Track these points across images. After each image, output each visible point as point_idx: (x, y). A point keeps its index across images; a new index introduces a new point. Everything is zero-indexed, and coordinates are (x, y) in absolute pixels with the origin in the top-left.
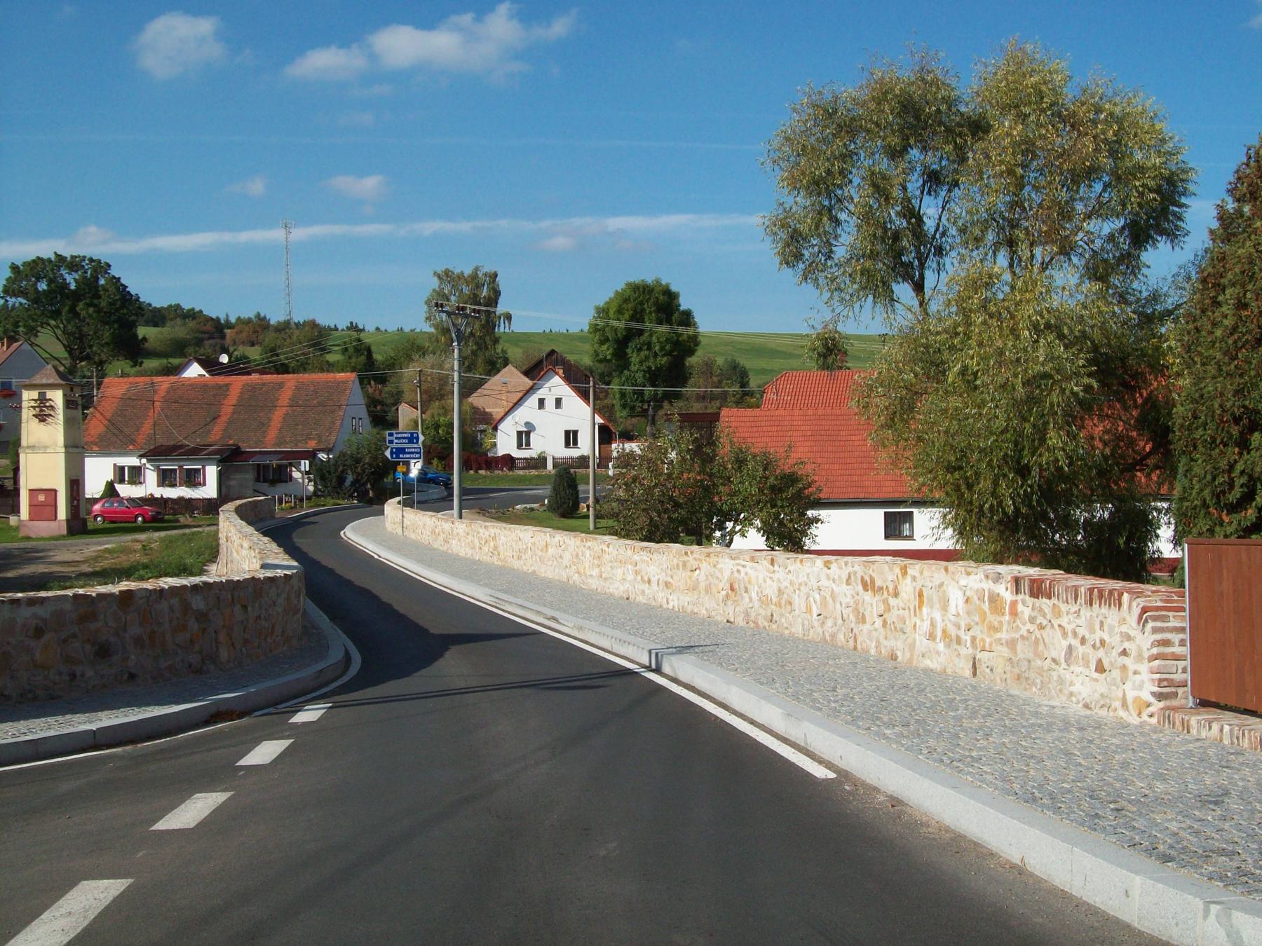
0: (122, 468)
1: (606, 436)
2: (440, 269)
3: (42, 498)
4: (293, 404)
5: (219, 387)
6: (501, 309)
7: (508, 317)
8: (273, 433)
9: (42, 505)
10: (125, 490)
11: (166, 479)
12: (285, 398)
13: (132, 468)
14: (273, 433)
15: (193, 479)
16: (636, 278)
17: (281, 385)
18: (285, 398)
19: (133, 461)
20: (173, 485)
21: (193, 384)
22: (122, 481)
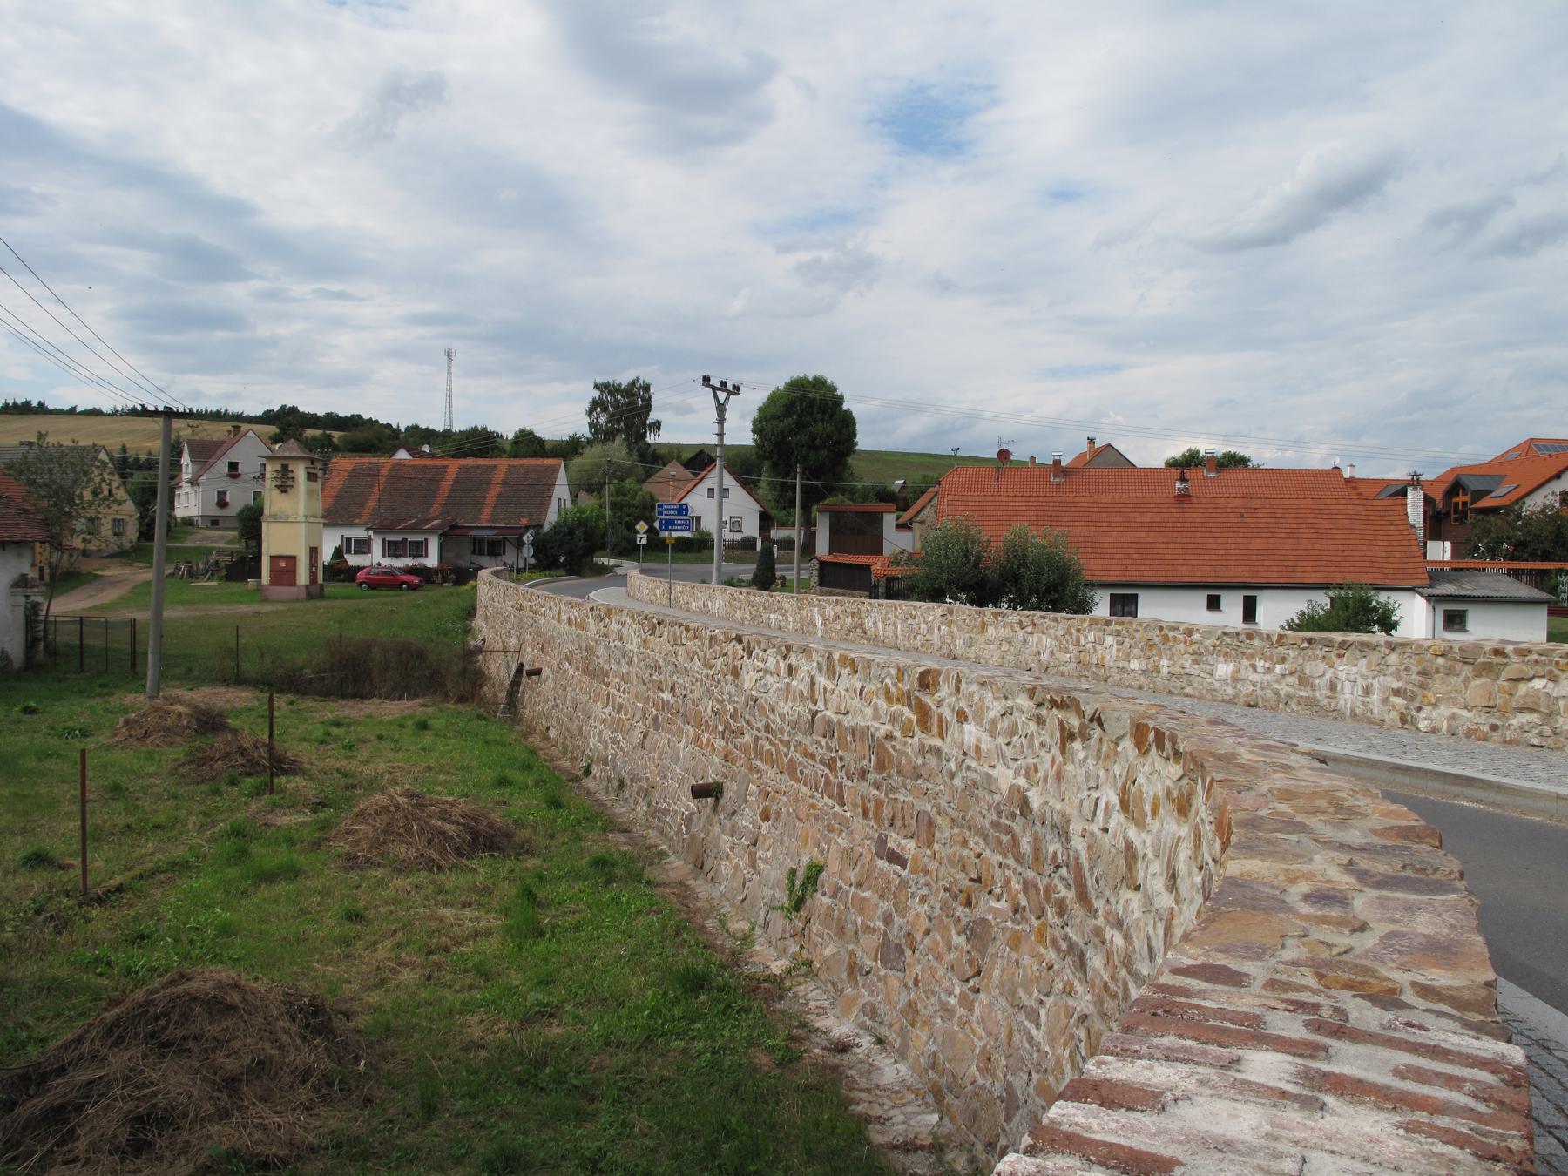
0: (349, 540)
1: (766, 521)
2: (600, 380)
3: (283, 564)
4: (505, 484)
5: (437, 468)
6: (653, 417)
7: (657, 425)
8: (487, 511)
9: (282, 571)
10: (353, 560)
11: (392, 550)
12: (498, 477)
13: (358, 542)
14: (487, 511)
15: (419, 549)
16: (798, 373)
17: (494, 468)
18: (498, 477)
19: (360, 533)
20: (397, 556)
21: (400, 464)
22: (349, 552)
